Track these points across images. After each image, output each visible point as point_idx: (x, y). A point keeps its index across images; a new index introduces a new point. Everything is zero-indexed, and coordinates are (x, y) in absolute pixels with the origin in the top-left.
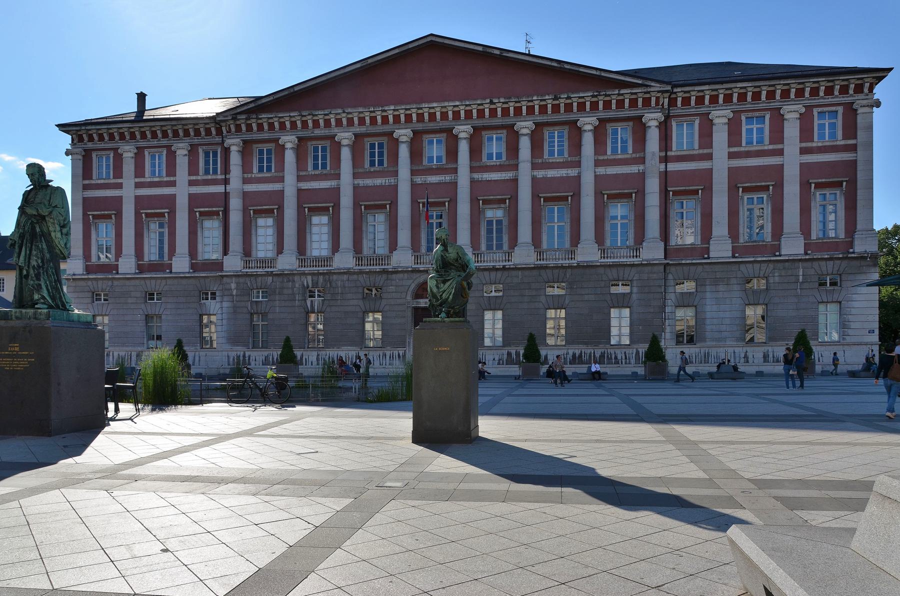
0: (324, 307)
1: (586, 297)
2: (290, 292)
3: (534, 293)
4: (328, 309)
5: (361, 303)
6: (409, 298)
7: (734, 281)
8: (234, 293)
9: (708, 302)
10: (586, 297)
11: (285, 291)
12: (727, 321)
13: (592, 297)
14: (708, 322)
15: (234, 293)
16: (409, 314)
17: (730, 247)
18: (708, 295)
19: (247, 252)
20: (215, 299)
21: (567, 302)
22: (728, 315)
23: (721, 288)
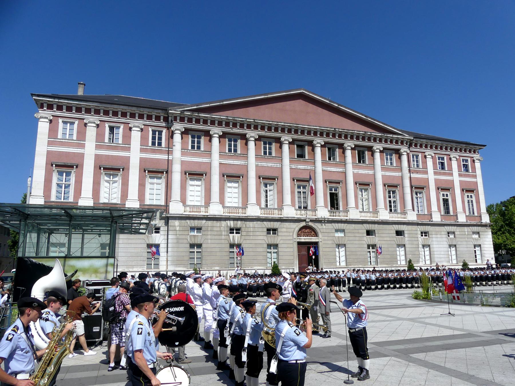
0: (242, 241)
1: (385, 239)
2: (218, 229)
3: (361, 235)
4: (244, 242)
5: (265, 238)
6: (295, 236)
7: (443, 233)
8: (178, 228)
9: (434, 243)
10: (385, 239)
11: (215, 229)
12: (442, 253)
13: (388, 239)
14: (435, 253)
15: (178, 228)
16: (296, 245)
17: (440, 216)
18: (434, 239)
19: (183, 201)
20: (158, 232)
21: (377, 241)
22: (442, 249)
23: (439, 236)
